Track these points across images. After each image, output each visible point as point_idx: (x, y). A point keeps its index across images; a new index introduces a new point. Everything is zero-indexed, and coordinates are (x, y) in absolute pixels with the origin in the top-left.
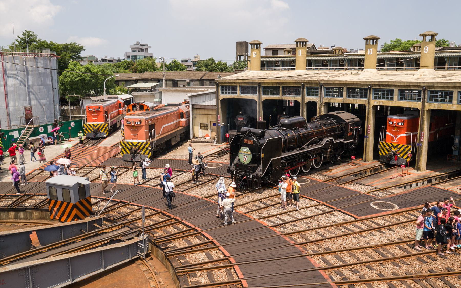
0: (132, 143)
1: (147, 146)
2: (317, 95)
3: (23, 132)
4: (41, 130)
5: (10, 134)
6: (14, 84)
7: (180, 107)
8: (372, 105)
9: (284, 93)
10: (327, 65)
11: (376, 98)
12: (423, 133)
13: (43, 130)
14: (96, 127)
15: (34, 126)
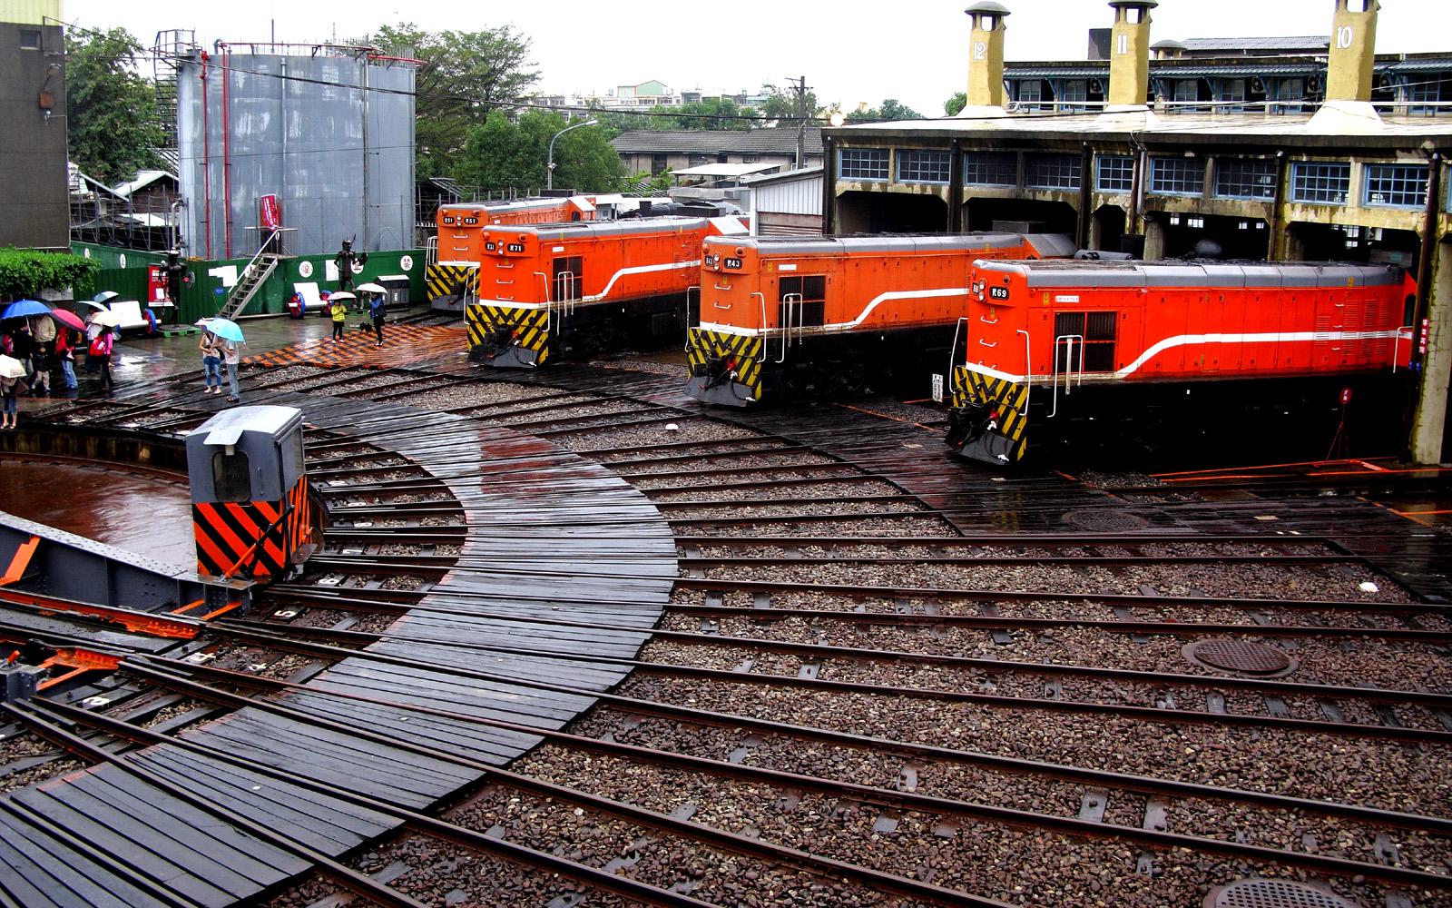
0: (498, 309)
1: (540, 323)
2: (1127, 186)
3: (247, 272)
4: (306, 269)
5: (212, 272)
6: (251, 134)
7: (714, 220)
8: (1287, 221)
9: (1033, 179)
10: (1262, 98)
11: (1299, 195)
12: (1425, 322)
13: (311, 272)
14: (462, 275)
15: (281, 257)
